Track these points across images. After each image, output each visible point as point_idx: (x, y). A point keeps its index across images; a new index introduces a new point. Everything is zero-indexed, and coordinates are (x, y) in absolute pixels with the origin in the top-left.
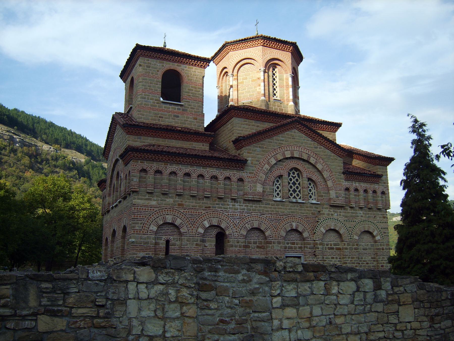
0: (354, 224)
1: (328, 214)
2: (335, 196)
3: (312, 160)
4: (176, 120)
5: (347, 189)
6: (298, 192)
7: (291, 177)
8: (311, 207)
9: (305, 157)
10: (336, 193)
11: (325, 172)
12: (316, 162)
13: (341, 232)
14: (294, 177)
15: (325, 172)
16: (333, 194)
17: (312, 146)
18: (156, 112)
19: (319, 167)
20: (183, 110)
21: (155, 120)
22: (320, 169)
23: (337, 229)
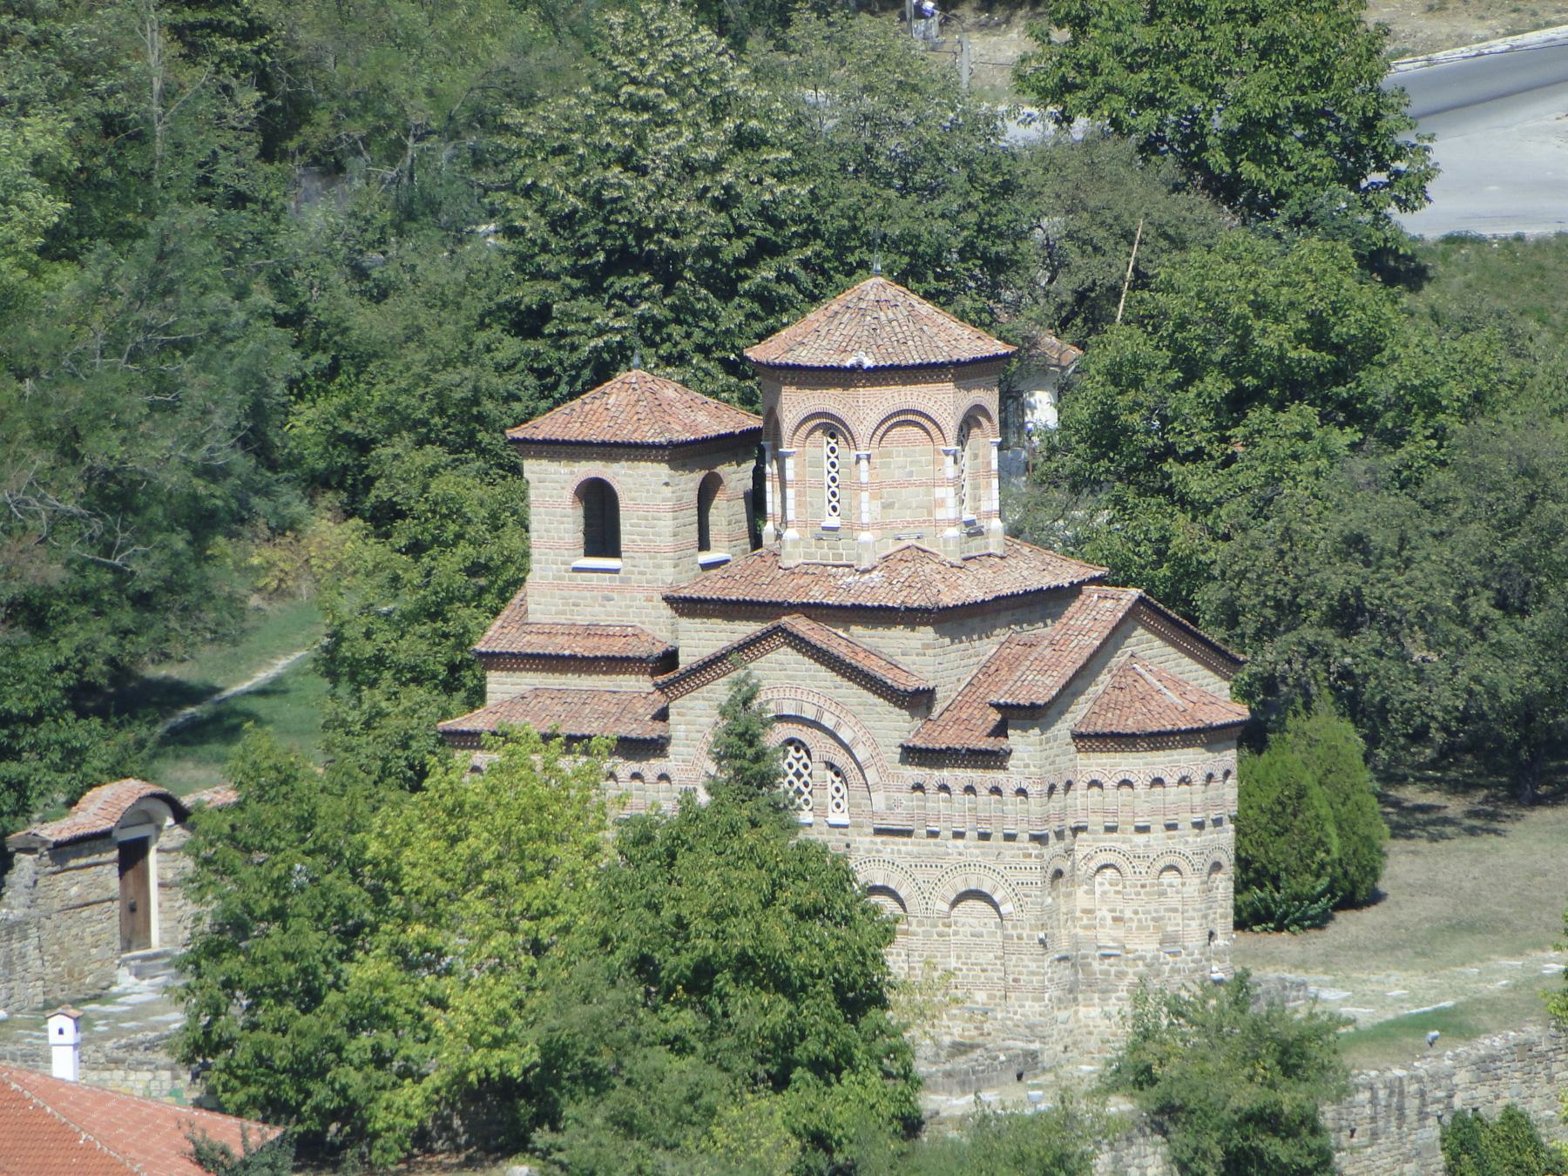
0: (938, 873)
1: (869, 851)
2: (883, 806)
3: (828, 721)
4: (610, 607)
5: (918, 787)
6: (806, 796)
7: (790, 759)
8: (829, 833)
9: (810, 714)
10: (887, 799)
11: (861, 746)
12: (838, 724)
13: (902, 894)
14: (798, 760)
15: (861, 746)
16: (879, 800)
17: (828, 684)
18: (566, 593)
19: (845, 735)
20: (622, 581)
21: (564, 613)
22: (846, 741)
23: (892, 886)
